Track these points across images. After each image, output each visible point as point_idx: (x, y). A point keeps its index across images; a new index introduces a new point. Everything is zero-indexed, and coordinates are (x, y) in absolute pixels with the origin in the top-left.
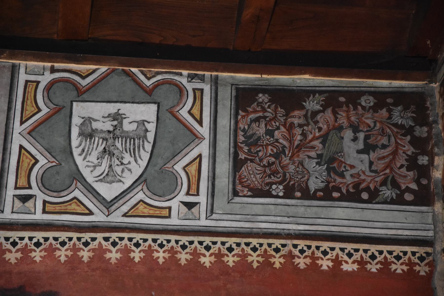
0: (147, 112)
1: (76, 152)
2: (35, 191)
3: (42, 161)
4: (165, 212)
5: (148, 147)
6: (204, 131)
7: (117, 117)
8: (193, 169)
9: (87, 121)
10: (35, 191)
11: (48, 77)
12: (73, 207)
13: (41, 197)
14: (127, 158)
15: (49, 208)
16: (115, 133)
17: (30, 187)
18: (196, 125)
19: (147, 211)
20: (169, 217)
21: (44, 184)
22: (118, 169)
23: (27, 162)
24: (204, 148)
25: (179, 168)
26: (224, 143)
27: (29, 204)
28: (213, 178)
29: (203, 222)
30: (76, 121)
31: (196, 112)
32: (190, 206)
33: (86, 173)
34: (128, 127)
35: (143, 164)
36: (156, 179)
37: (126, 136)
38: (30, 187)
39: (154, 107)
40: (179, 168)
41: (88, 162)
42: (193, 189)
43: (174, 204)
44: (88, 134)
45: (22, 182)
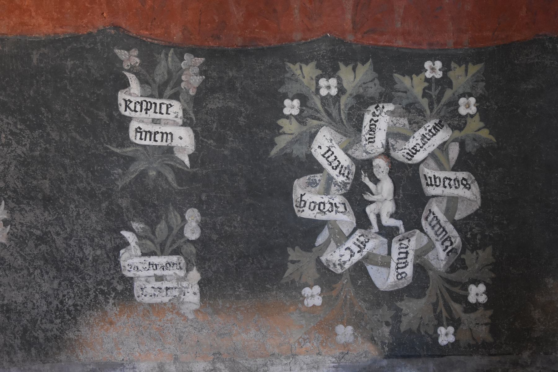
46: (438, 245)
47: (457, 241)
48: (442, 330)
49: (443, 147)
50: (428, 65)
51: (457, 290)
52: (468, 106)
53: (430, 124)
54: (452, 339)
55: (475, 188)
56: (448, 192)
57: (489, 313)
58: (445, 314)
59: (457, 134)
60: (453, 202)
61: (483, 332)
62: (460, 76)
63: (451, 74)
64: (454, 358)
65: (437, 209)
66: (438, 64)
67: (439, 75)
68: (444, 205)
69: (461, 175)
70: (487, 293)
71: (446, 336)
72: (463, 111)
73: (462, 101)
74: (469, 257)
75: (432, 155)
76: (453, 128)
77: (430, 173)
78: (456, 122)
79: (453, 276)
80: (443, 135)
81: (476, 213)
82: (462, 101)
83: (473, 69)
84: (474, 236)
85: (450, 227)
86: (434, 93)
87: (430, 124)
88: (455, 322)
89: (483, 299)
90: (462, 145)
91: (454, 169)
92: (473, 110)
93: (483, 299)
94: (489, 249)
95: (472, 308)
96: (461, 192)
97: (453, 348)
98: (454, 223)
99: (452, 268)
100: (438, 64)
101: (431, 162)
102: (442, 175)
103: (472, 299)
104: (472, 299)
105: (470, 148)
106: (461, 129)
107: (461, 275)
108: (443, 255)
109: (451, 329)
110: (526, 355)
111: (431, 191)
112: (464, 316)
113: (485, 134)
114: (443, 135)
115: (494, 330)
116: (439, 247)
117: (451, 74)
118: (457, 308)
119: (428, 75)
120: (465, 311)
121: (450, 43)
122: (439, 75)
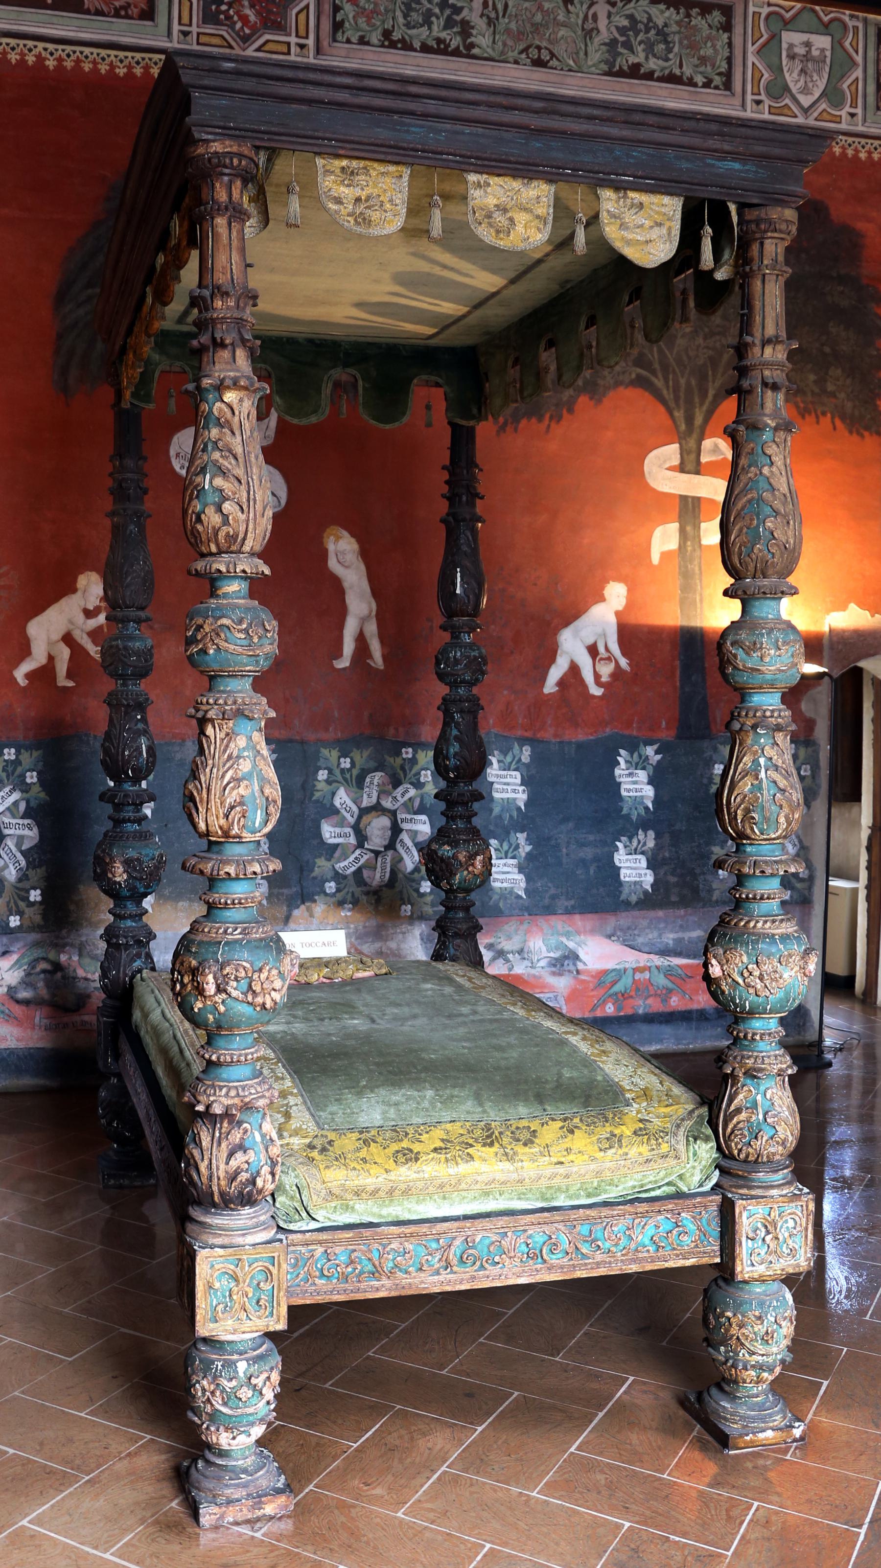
0: (822, 42)
1: (785, 69)
2: (763, 97)
3: (766, 75)
4: (838, 119)
5: (827, 69)
6: (859, 59)
7: (808, 44)
8: (853, 88)
9: (791, 46)
10: (763, 97)
11: (765, 11)
12: (786, 111)
13: (767, 102)
14: (815, 77)
15: (773, 110)
16: (807, 57)
17: (760, 94)
18: (854, 54)
19: (828, 117)
20: (840, 122)
21: (769, 95)
22: (810, 85)
23: (757, 75)
24: (859, 73)
25: (845, 86)
26: (871, 70)
27: (761, 106)
28: (865, 96)
29: (860, 128)
30: (784, 46)
31: (854, 44)
32: (853, 115)
33: (791, 85)
34: (815, 53)
35: (825, 81)
36: (833, 95)
37: (814, 60)
38: (760, 94)
39: (829, 39)
40: (845, 86)
41: (792, 78)
42: (854, 105)
43: (843, 113)
44: (792, 57)
45: (756, 90)
46: (11, 866)
47: (23, 863)
48: (12, 918)
49: (16, 804)
50: (6, 751)
51: (23, 893)
52: (32, 777)
53: (7, 789)
54: (18, 923)
55: (36, 830)
56: (18, 832)
57: (42, 907)
58: (14, 908)
59: (25, 795)
60: (20, 839)
61: (38, 919)
62: (27, 758)
63: (21, 757)
64: (19, 935)
65: (10, 843)
66: (13, 750)
67: (13, 757)
68: (15, 841)
69: (26, 821)
70: (41, 895)
71: (14, 921)
72: (28, 780)
73: (28, 774)
74: (31, 873)
75: (8, 809)
76: (22, 791)
77: (6, 820)
78: (25, 788)
79: (20, 885)
80: (16, 796)
81: (36, 846)
82: (28, 774)
83: (36, 754)
84: (34, 860)
85: (19, 855)
86: (10, 769)
87: (7, 789)
88: (20, 913)
89: (39, 899)
90: (28, 802)
91: (22, 818)
92: (35, 780)
93: (39, 899)
94: (44, 868)
95: (33, 904)
96: (27, 832)
97: (19, 929)
98: (22, 852)
99: (20, 880)
100: (13, 750)
101: (8, 814)
102: (14, 821)
103: (32, 899)
104: (32, 899)
105: (33, 804)
106: (27, 792)
107: (26, 885)
108: (14, 872)
109: (18, 918)
110: (64, 932)
111: (6, 832)
112: (27, 910)
113: (42, 795)
114: (16, 796)
115: (45, 916)
116: (11, 867)
117: (21, 757)
118: (22, 904)
119: (6, 757)
120: (28, 906)
121: (21, 737)
122: (13, 757)
